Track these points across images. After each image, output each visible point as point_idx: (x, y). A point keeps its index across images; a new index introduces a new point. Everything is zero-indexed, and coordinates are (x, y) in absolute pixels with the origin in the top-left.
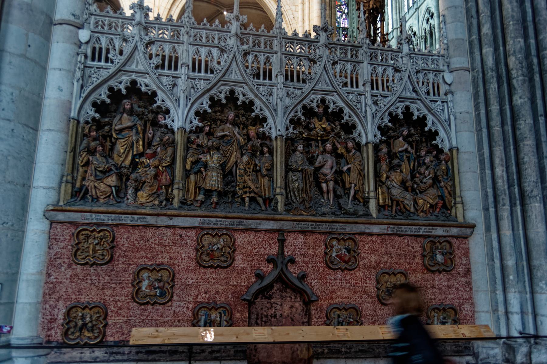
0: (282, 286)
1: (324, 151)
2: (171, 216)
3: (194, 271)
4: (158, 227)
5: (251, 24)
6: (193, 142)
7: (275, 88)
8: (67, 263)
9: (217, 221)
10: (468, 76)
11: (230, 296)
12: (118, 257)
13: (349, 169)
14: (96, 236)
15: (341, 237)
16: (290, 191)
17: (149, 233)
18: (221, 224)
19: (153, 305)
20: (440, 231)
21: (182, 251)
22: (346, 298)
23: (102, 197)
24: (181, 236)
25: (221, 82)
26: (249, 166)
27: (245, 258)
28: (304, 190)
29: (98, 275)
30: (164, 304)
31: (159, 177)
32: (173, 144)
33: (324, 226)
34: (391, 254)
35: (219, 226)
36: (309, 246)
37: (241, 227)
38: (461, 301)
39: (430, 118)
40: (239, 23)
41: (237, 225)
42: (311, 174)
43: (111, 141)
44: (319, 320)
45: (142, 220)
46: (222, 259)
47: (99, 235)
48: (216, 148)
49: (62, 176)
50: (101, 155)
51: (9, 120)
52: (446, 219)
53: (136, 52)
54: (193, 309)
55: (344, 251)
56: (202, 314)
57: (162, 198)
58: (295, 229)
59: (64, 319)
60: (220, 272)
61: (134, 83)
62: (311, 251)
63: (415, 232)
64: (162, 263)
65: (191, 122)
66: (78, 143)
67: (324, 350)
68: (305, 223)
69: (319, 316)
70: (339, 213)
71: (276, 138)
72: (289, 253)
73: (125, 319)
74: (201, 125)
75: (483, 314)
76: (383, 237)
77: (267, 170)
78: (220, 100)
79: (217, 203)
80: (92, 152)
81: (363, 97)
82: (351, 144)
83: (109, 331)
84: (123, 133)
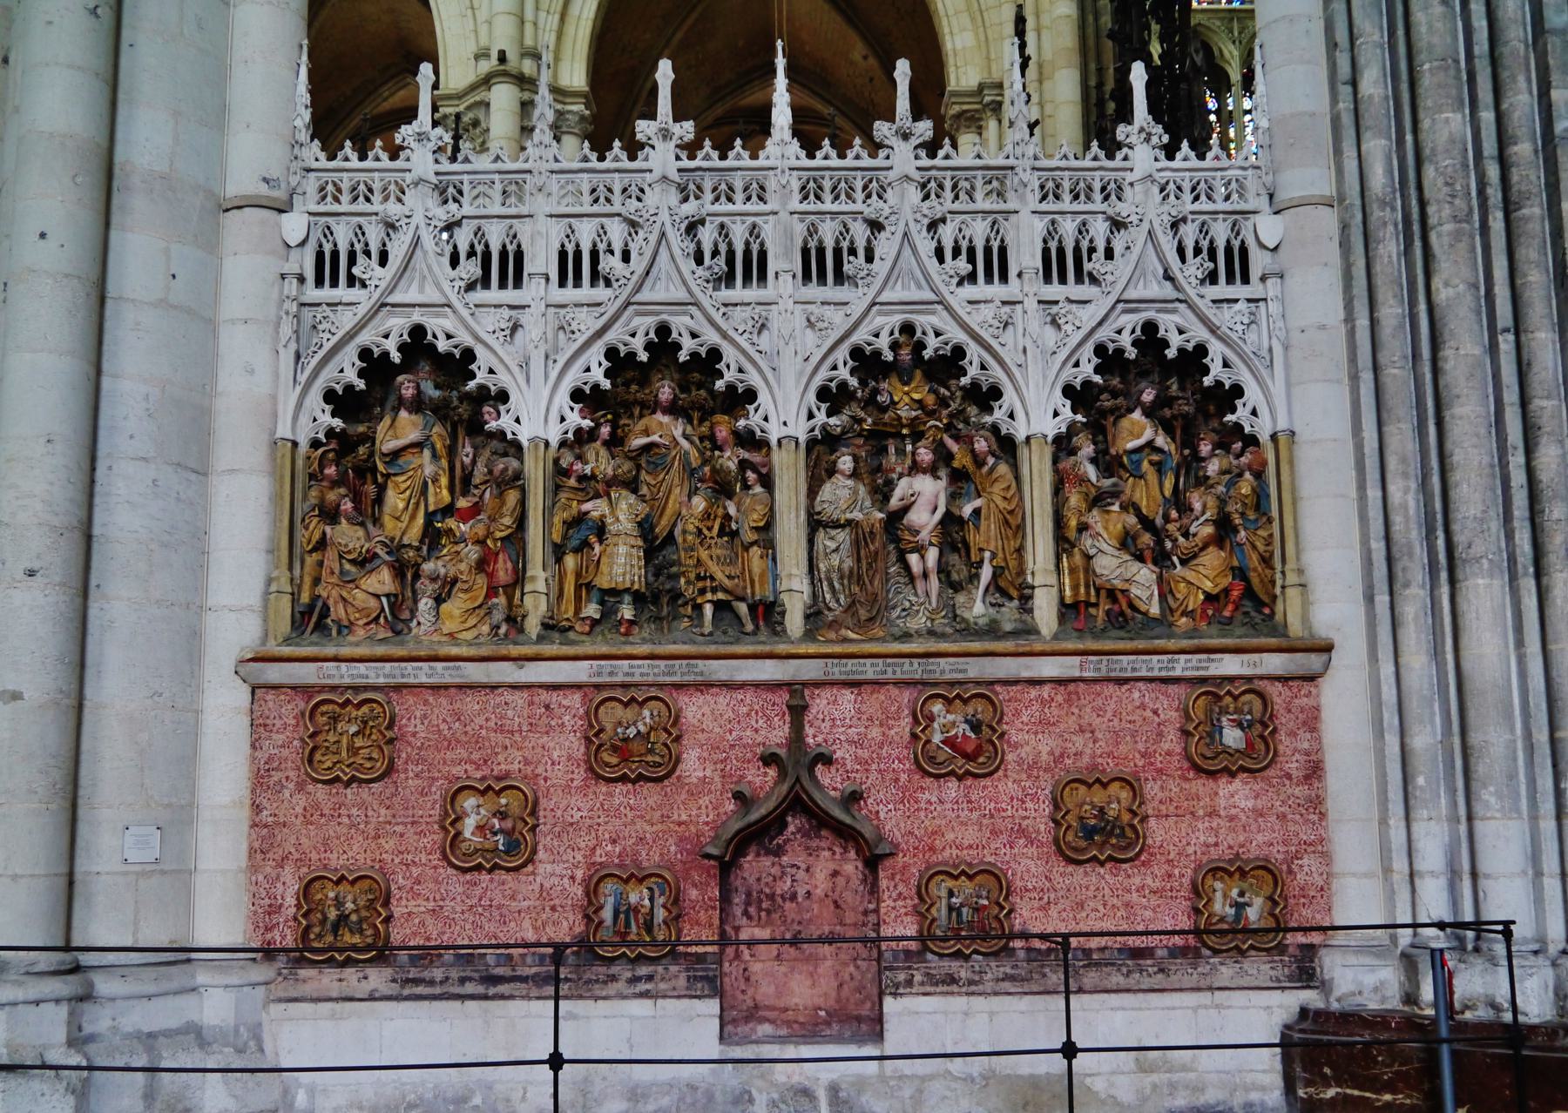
0: (809, 821)
4: (494, 687)
5: (707, 143)
6: (566, 473)
8: (295, 779)
9: (631, 667)
10: (1328, 220)
12: (406, 763)
13: (977, 512)
14: (354, 713)
15: (955, 693)
16: (820, 580)
17: (470, 703)
18: (642, 675)
19: (490, 871)
20: (1230, 665)
21: (551, 745)
22: (970, 847)
23: (361, 622)
24: (547, 707)
25: (631, 308)
26: (710, 524)
27: (705, 754)
29: (363, 805)
31: (489, 565)
32: (516, 480)
33: (906, 667)
34: (1092, 732)
35: (637, 678)
36: (870, 719)
37: (692, 678)
38: (1293, 848)
39: (1216, 349)
40: (672, 144)
41: (683, 674)
42: (871, 532)
43: (375, 481)
44: (900, 903)
45: (453, 673)
46: (650, 758)
47: (360, 713)
49: (269, 581)
50: (350, 521)
51: (144, 459)
52: (1252, 632)
53: (418, 252)
54: (586, 882)
55: (963, 728)
56: (607, 892)
57: (498, 616)
58: (830, 677)
59: (299, 906)
60: (645, 792)
61: (418, 331)
62: (875, 732)
64: (506, 775)
65: (563, 419)
66: (299, 495)
67: (913, 976)
68: (856, 661)
69: (900, 894)
70: (949, 630)
71: (779, 441)
72: (820, 739)
73: (431, 905)
74: (587, 423)
75: (1351, 881)
76: (1071, 687)
77: (757, 529)
78: (632, 355)
79: (631, 623)
81: (1019, 307)
82: (984, 443)
84: (401, 461)
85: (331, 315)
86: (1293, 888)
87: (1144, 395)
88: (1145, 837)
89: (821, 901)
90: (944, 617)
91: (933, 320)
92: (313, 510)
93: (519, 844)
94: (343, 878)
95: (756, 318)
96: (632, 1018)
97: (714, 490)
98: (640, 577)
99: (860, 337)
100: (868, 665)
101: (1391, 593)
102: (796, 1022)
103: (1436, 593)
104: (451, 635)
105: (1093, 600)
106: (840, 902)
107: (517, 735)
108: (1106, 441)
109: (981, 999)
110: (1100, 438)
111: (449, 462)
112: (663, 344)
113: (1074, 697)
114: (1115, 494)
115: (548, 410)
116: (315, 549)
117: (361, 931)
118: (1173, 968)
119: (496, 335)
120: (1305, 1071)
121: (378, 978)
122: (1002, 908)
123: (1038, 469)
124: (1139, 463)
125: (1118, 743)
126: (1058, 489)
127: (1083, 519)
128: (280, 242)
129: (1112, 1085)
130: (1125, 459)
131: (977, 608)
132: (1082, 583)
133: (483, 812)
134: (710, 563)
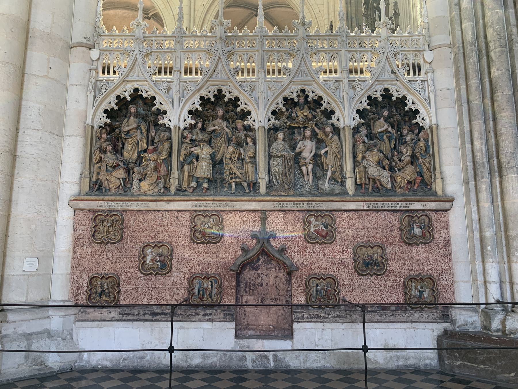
0: (267, 258)
1: (304, 138)
2: (168, 201)
3: (189, 246)
4: (159, 211)
6: (185, 138)
7: (257, 82)
9: (207, 204)
11: (220, 267)
13: (326, 152)
15: (319, 214)
16: (272, 175)
18: (210, 206)
19: (155, 275)
20: (417, 206)
21: (178, 230)
22: (324, 268)
23: (113, 188)
24: (177, 217)
26: (234, 156)
27: (232, 234)
28: (284, 174)
30: (165, 274)
31: (158, 169)
33: (301, 205)
34: (367, 229)
35: (209, 208)
37: (227, 208)
45: (144, 205)
47: (112, 219)
48: (205, 141)
52: (424, 194)
53: (137, 63)
54: (189, 278)
55: (321, 227)
57: (161, 186)
60: (211, 247)
61: (136, 90)
63: (392, 207)
65: (185, 120)
66: (94, 144)
67: (304, 315)
68: (284, 202)
69: (299, 285)
70: (316, 192)
71: (258, 128)
72: (271, 229)
74: (193, 122)
76: (360, 213)
78: (209, 99)
79: (207, 189)
80: (103, 151)
81: (341, 83)
83: (122, 297)
85: (107, 84)
86: (440, 286)
87: (384, 113)
88: (387, 267)
89: (271, 286)
90: (314, 188)
91: (312, 87)
93: (166, 266)
94: (103, 277)
95: (251, 86)
96: (204, 329)
97: (236, 144)
98: (210, 173)
99: (286, 94)
100: (288, 204)
101: (475, 180)
102: (262, 330)
103: (493, 180)
104: (144, 192)
105: (367, 183)
106: (278, 287)
107: (166, 227)
108: (371, 129)
109: (328, 324)
110: (369, 128)
111: (147, 135)
112: (219, 95)
113: (361, 216)
114: (375, 146)
115: (180, 116)
116: (98, 163)
117: (109, 296)
118: (398, 314)
119: (163, 91)
120: (448, 354)
121: (115, 313)
122: (336, 291)
123: (347, 137)
124: (383, 136)
125: (377, 233)
126: (354, 145)
127: (364, 154)
128: (90, 60)
129: (376, 356)
130: (378, 135)
131: (326, 185)
132: (364, 176)
133: (153, 254)
134: (234, 169)
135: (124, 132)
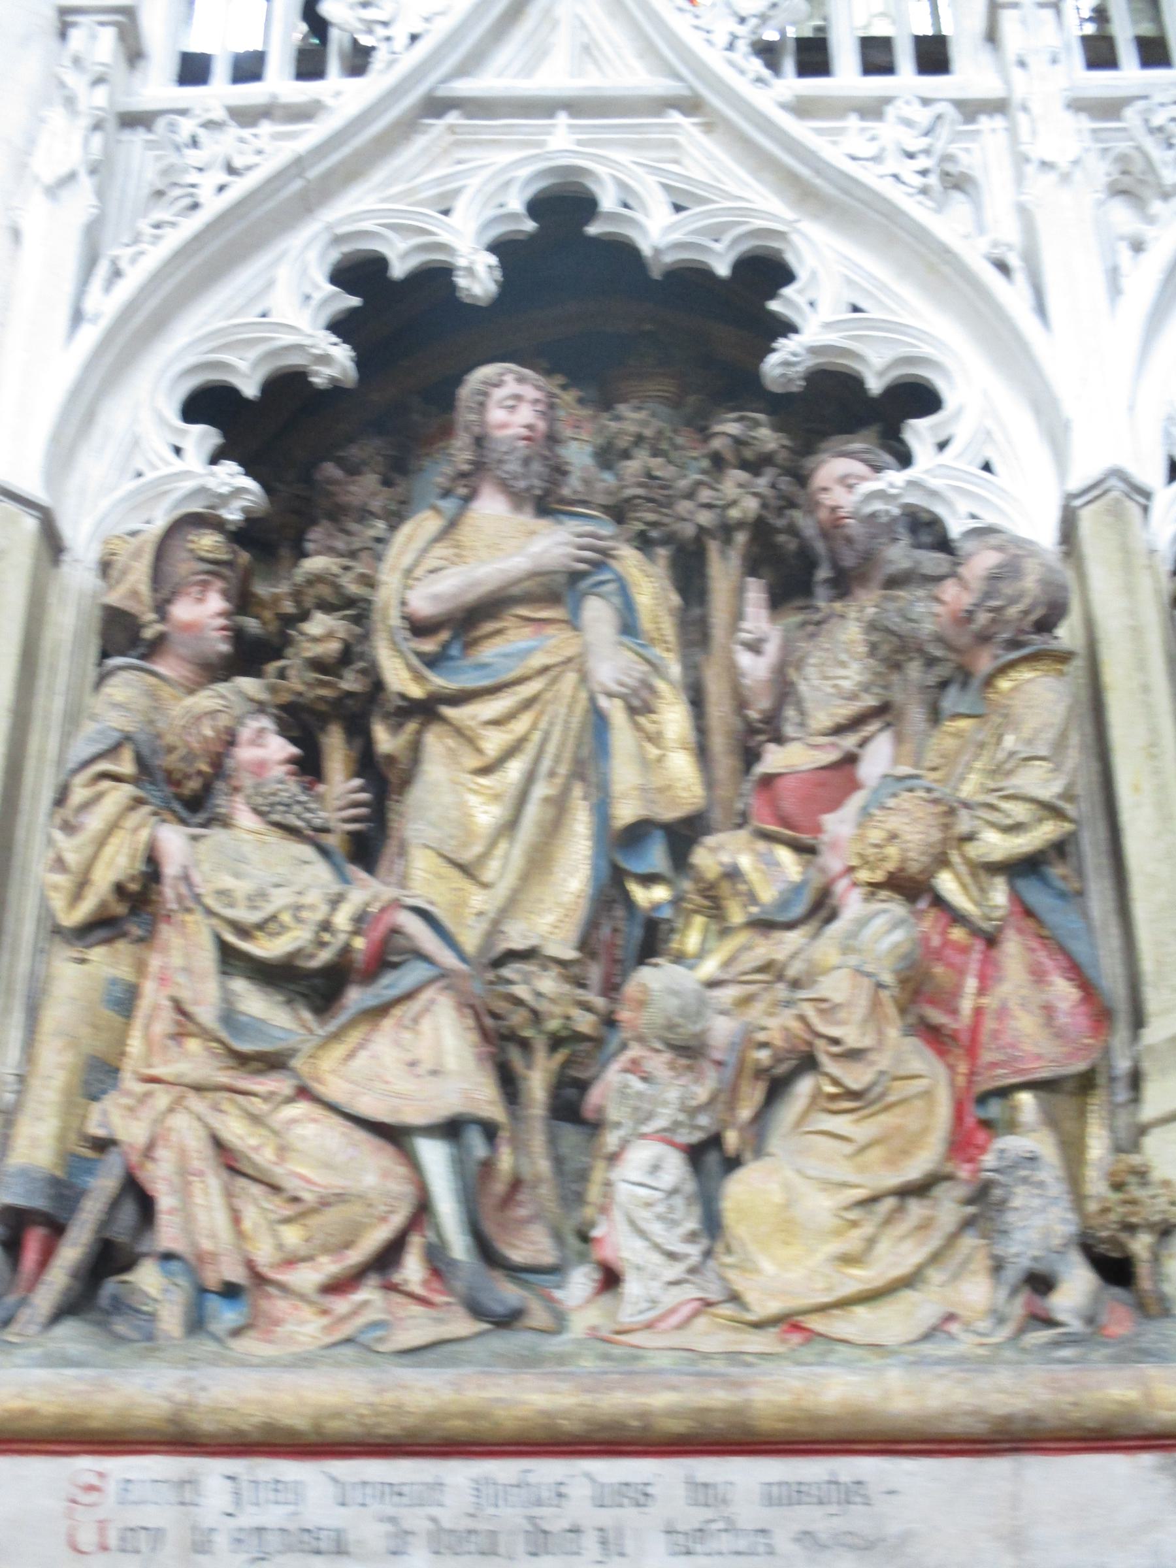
23: (307, 1277)
31: (948, 1001)
84: (488, 652)
92: (112, 752)
135: (419, 628)
